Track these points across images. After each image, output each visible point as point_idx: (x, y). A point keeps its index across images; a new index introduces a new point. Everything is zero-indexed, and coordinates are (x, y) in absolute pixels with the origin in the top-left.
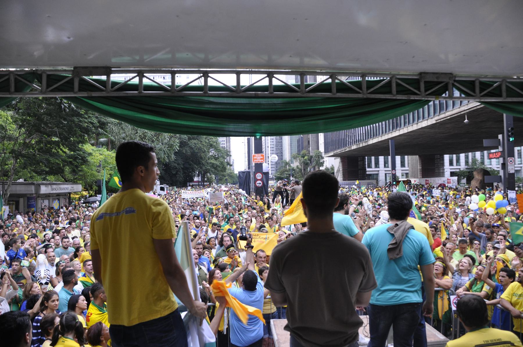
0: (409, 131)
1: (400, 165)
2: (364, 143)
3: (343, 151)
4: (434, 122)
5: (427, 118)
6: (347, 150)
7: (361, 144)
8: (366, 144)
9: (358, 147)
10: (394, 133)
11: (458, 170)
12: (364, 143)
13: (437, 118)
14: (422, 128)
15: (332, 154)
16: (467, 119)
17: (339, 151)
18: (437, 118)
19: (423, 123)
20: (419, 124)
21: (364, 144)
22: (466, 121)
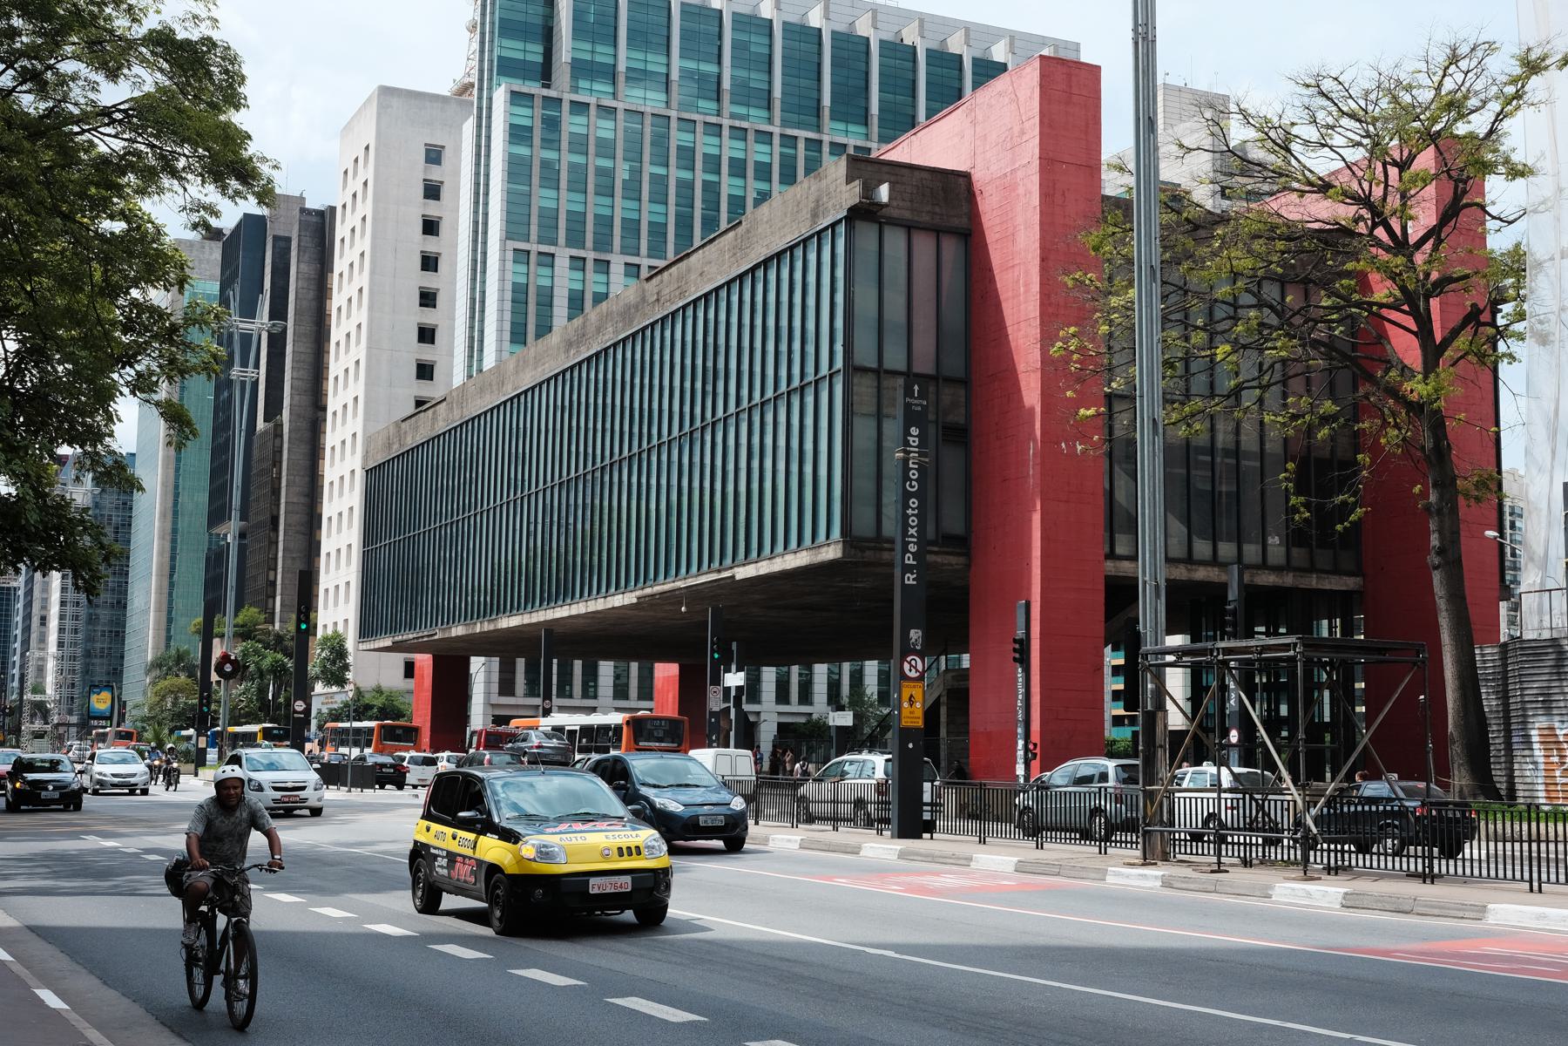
0: (589, 610)
1: (610, 692)
2: (486, 623)
3: (425, 639)
4: (635, 601)
5: (622, 590)
6: (436, 637)
7: (479, 625)
8: (492, 627)
9: (470, 632)
11: (802, 720)
12: (486, 623)
13: (639, 593)
14: (613, 608)
15: (388, 642)
17: (411, 636)
18: (639, 593)
20: (609, 598)
22: (683, 609)
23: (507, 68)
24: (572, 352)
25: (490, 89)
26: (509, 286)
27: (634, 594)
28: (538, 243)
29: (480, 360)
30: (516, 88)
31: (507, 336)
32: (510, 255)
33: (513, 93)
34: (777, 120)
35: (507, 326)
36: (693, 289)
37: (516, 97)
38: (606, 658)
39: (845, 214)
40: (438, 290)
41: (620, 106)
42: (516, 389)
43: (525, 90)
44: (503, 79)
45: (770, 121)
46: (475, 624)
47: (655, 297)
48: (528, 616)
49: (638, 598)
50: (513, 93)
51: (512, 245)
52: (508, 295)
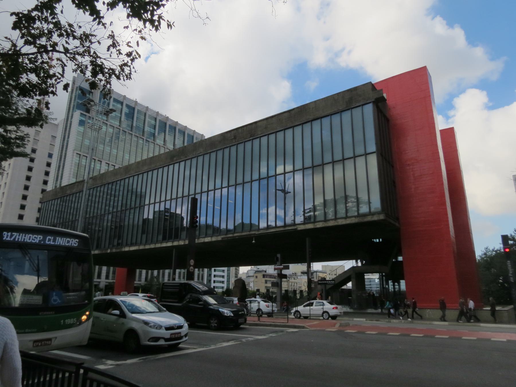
8: (118, 250)
10: (165, 243)
11: (139, 285)
16: (255, 241)
19: (206, 239)
21: (114, 250)
22: (254, 242)
23: (79, 107)
24: (175, 159)
25: (73, 112)
26: (74, 162)
27: (219, 237)
28: (83, 153)
29: (61, 182)
30: (82, 112)
31: (72, 175)
32: (75, 154)
33: (81, 113)
34: (145, 136)
35: (72, 173)
36: (260, 133)
37: (82, 114)
38: (105, 266)
39: (373, 100)
40: (33, 167)
41: (109, 123)
42: (137, 172)
43: (84, 113)
44: (77, 110)
45: (143, 135)
46: (107, 249)
47: (233, 137)
48: (160, 244)
49: (222, 238)
50: (81, 113)
51: (76, 152)
52: (73, 165)
